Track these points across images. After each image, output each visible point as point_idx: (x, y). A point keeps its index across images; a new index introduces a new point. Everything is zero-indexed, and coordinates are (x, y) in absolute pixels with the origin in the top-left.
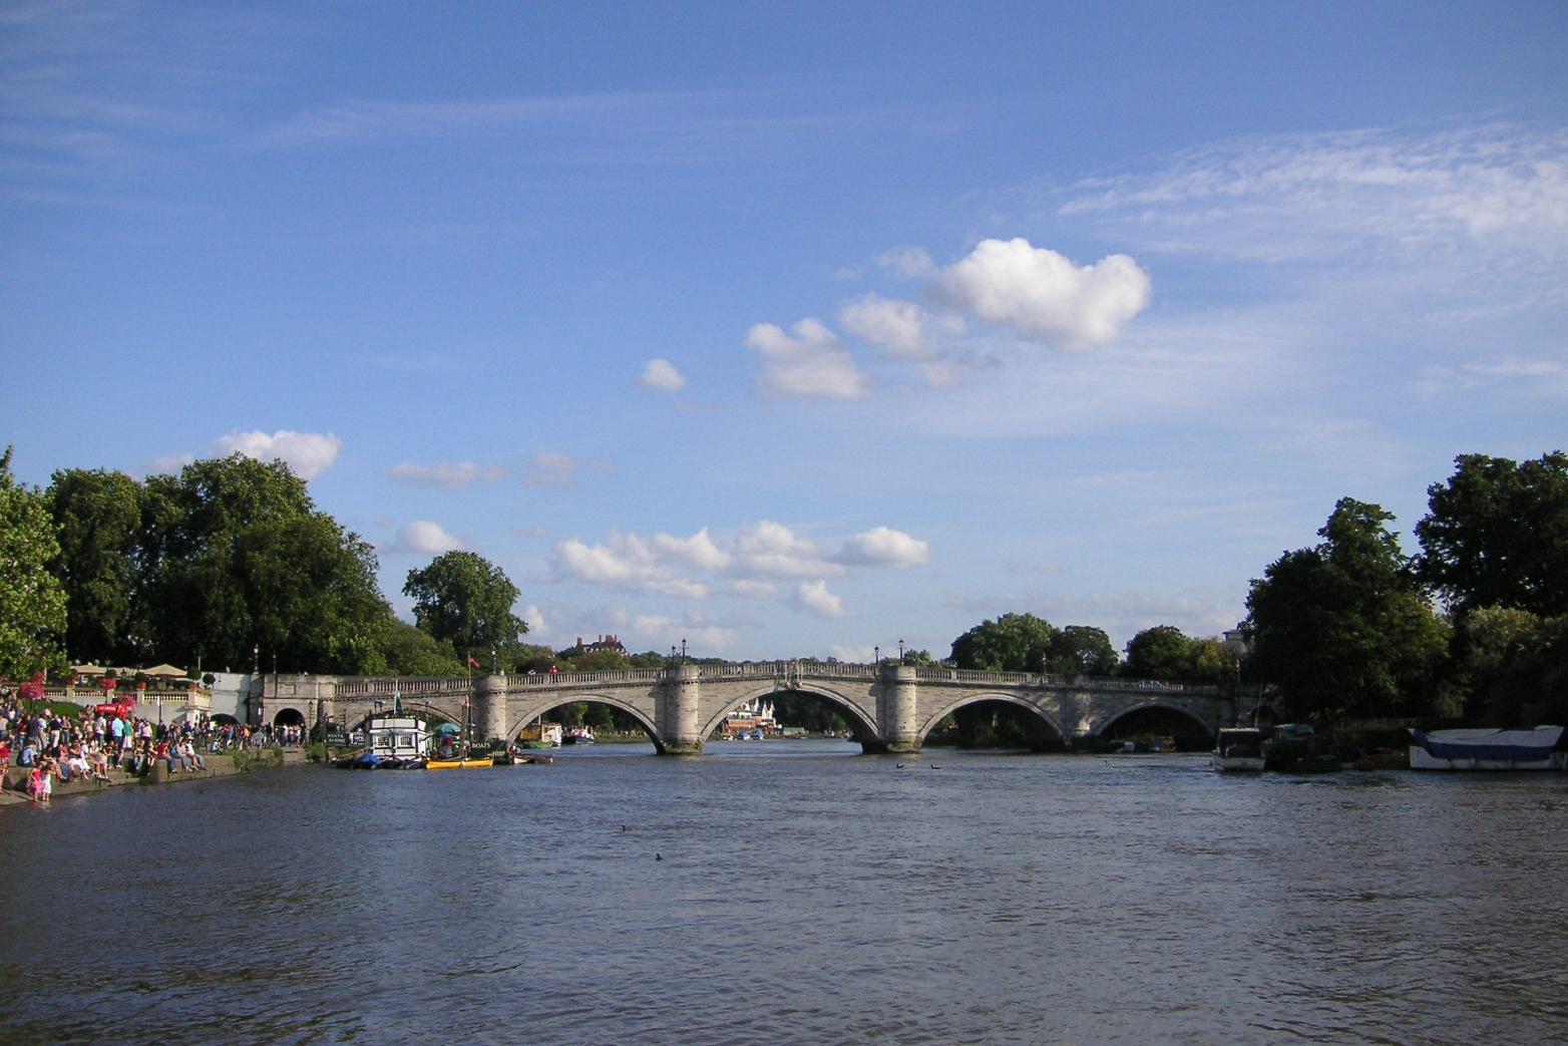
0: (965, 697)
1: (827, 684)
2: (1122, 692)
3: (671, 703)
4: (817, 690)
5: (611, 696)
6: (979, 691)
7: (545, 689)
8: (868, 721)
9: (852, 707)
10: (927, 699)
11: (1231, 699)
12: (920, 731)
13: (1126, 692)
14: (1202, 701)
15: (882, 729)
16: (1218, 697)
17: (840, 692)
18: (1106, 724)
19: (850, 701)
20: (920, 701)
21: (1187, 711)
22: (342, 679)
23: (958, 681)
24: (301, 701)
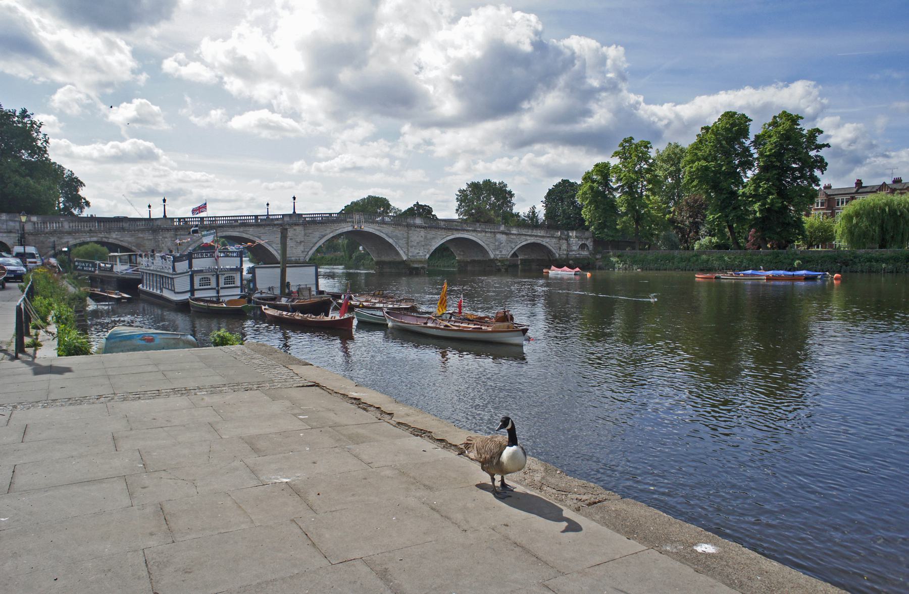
0: (448, 236)
1: (376, 227)
2: (521, 235)
4: (371, 230)
6: (455, 232)
8: (399, 249)
9: (390, 241)
11: (567, 240)
12: (426, 255)
13: (522, 235)
14: (554, 240)
15: (407, 255)
16: (560, 238)
17: (383, 231)
18: (513, 252)
19: (390, 237)
20: (426, 237)
21: (547, 245)
22: (40, 219)
24: (5, 235)
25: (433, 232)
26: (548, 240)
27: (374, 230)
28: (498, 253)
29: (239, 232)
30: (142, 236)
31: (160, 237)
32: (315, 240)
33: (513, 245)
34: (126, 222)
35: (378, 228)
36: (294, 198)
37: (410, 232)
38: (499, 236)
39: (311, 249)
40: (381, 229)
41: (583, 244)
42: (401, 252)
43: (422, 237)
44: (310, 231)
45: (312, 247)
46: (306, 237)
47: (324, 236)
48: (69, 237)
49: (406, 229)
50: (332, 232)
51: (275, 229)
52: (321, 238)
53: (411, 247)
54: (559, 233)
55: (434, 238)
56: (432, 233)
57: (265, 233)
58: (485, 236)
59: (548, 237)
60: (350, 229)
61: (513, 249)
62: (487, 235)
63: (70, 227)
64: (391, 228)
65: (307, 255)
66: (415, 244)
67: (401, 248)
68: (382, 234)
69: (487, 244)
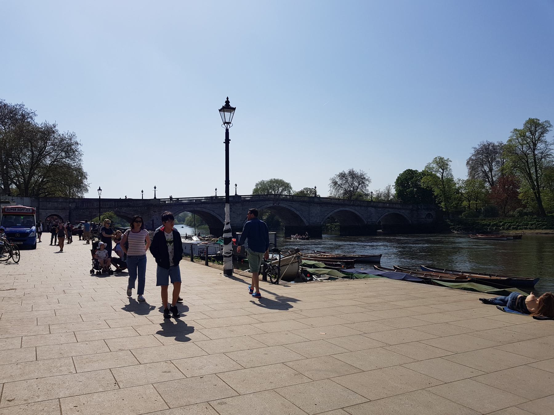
4: (285, 206)
9: (298, 213)
12: (321, 222)
26: (404, 211)
27: (287, 206)
28: (369, 220)
29: (201, 207)
36: (236, 185)
38: (370, 209)
41: (428, 213)
42: (305, 220)
43: (318, 210)
54: (411, 207)
59: (404, 209)
60: (272, 205)
67: (305, 218)
68: (292, 208)
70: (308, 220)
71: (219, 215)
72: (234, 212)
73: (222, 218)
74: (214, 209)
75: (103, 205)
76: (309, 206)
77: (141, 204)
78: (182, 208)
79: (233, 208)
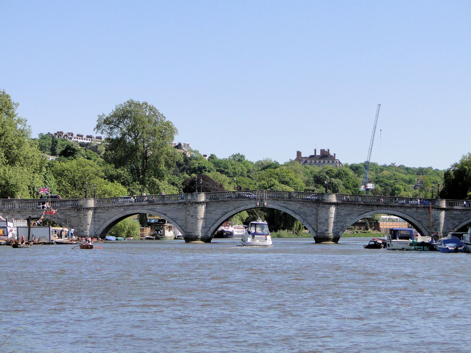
1: (281, 203)
3: (189, 215)
5: (155, 210)
7: (116, 206)
10: (343, 213)
15: (316, 232)
17: (290, 208)
23: (362, 203)
25: (349, 209)
30: (69, 213)
31: (82, 215)
32: (217, 217)
33: (456, 222)
34: (58, 203)
35: (284, 205)
37: (319, 208)
39: (213, 225)
40: (287, 205)
44: (212, 209)
45: (214, 223)
46: (209, 214)
47: (226, 213)
48: (19, 215)
49: (316, 205)
50: (235, 209)
51: (179, 207)
52: (223, 215)
53: (320, 224)
55: (348, 215)
56: (345, 211)
57: (170, 211)
58: (417, 212)
60: (253, 206)
61: (457, 226)
62: (419, 211)
63: (19, 207)
64: (299, 205)
65: (209, 231)
66: (323, 221)
69: (419, 221)
70: (316, 229)
71: (173, 220)
72: (192, 216)
73: (177, 224)
74: (166, 211)
75: (26, 206)
76: (318, 207)
77: (70, 205)
78: (123, 210)
79: (190, 211)
